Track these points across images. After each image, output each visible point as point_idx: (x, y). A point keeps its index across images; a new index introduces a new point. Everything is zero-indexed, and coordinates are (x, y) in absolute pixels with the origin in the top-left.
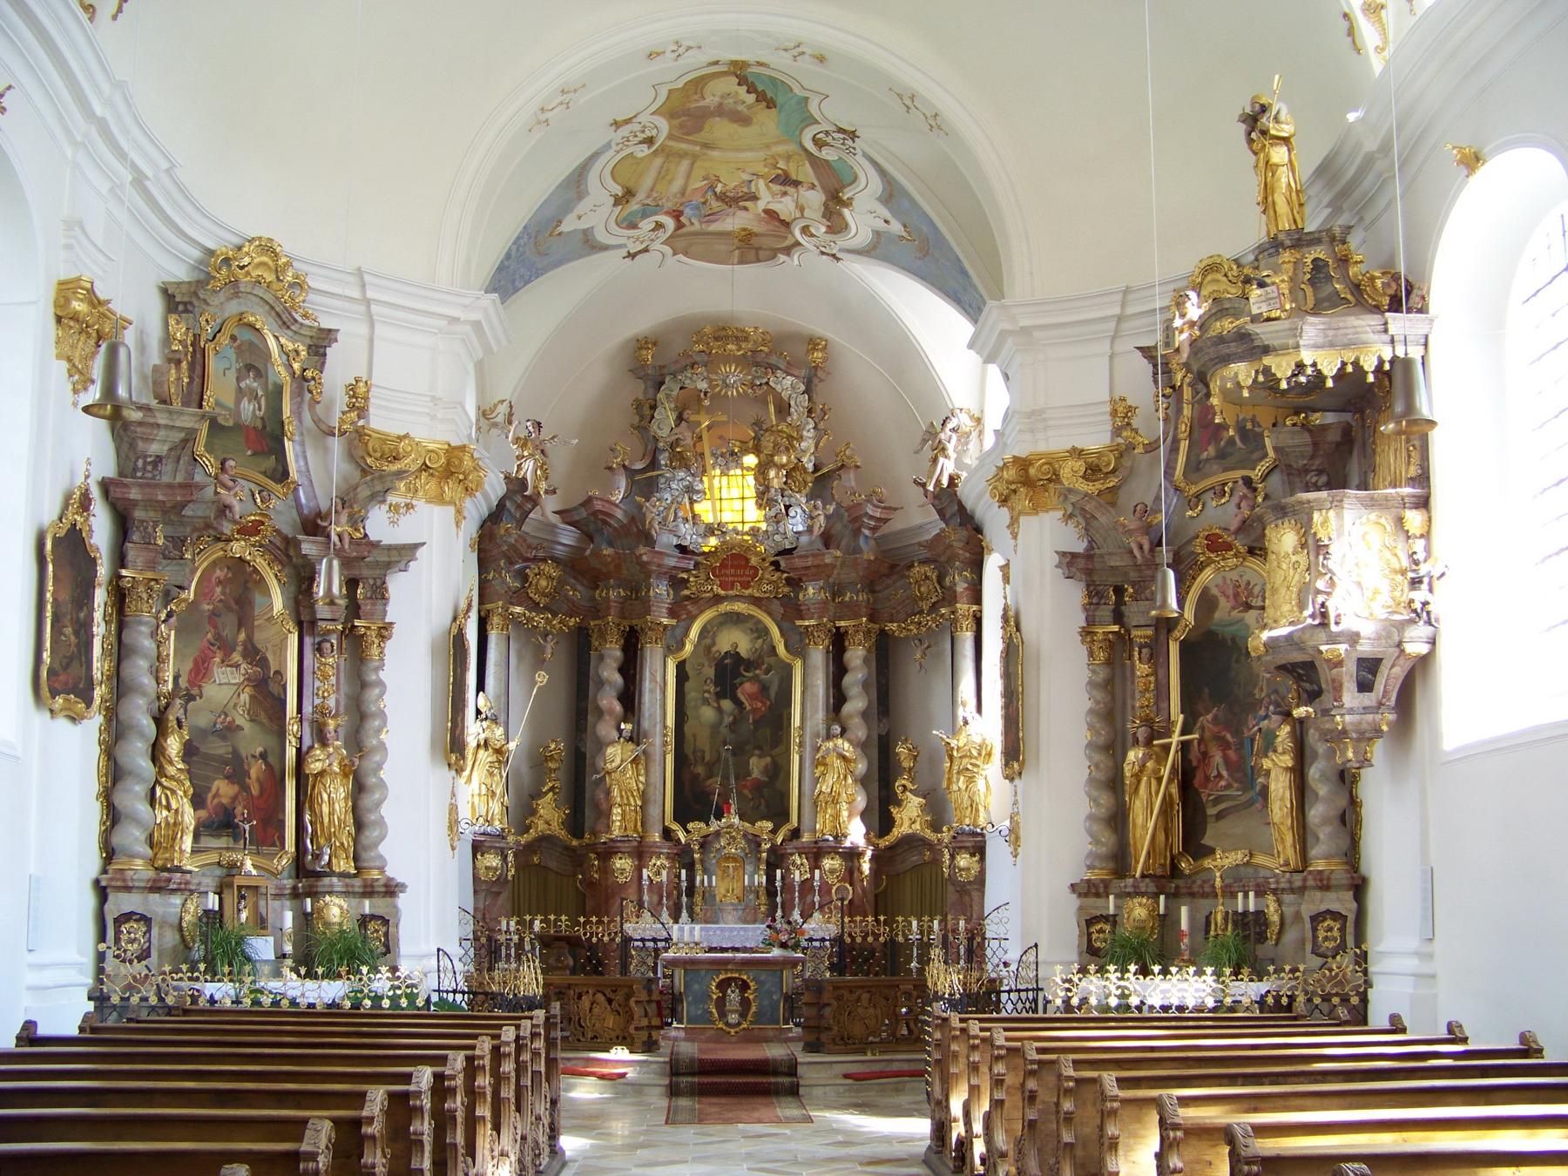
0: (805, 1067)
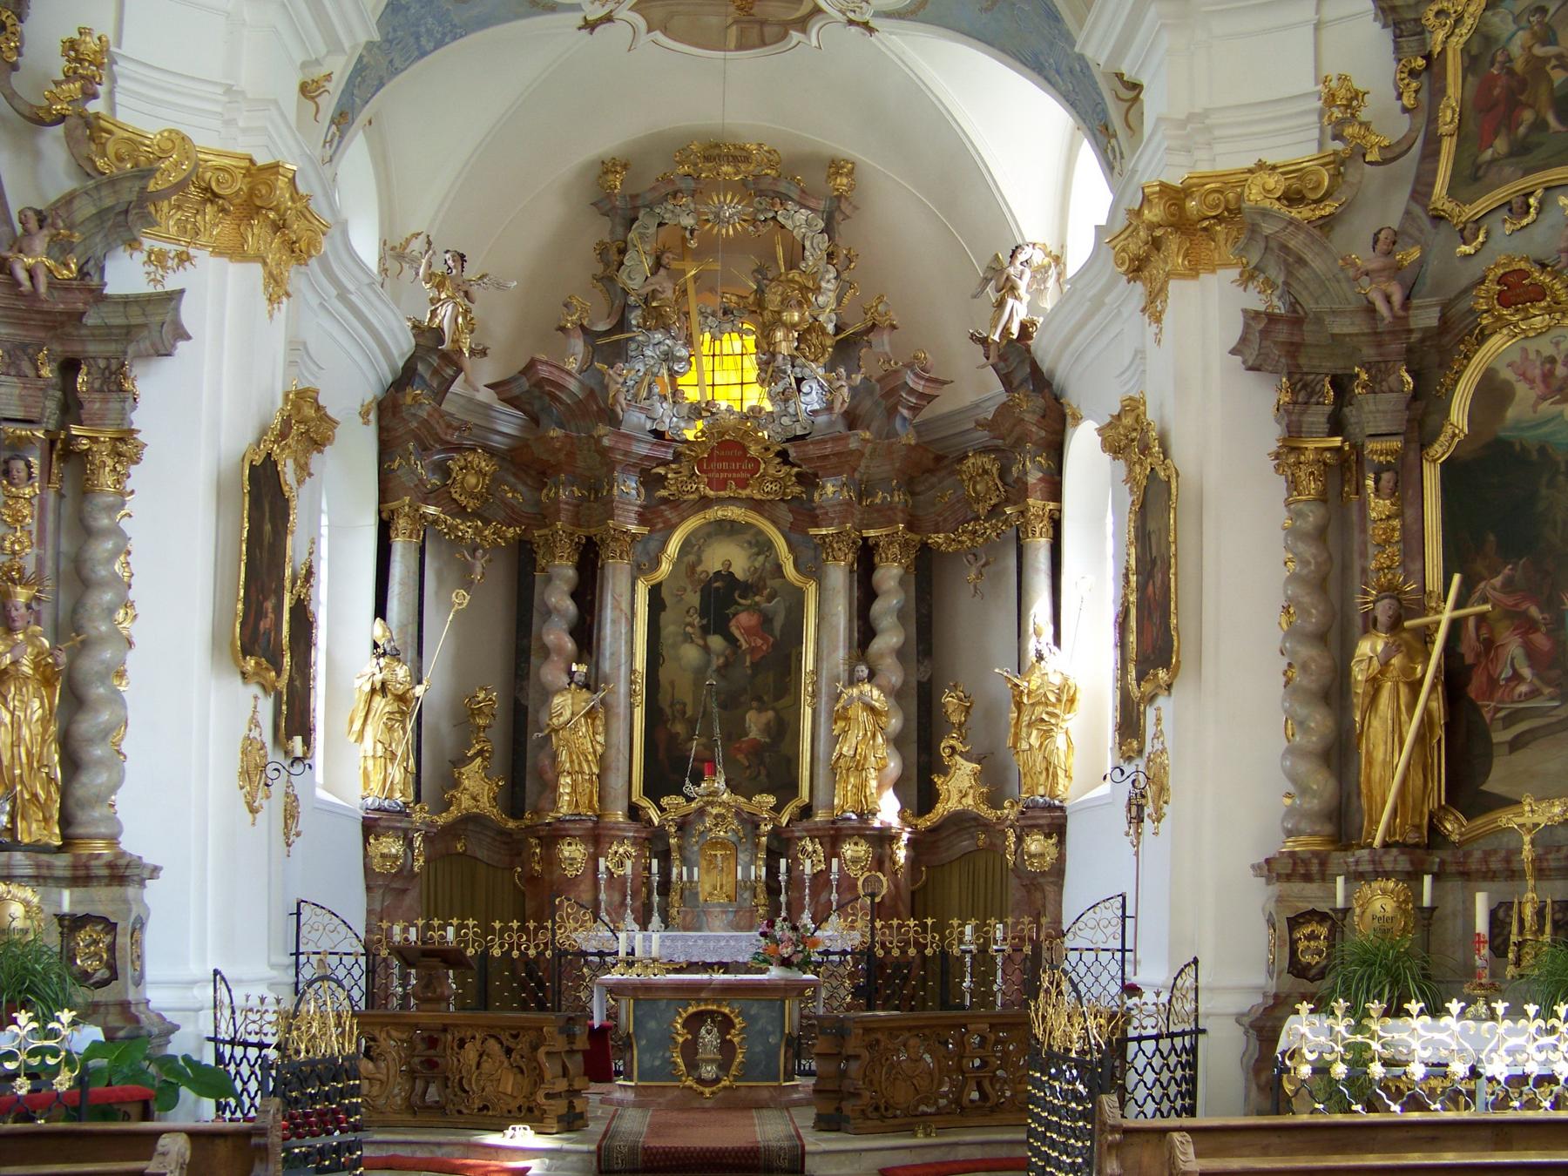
0: (817, 1158)
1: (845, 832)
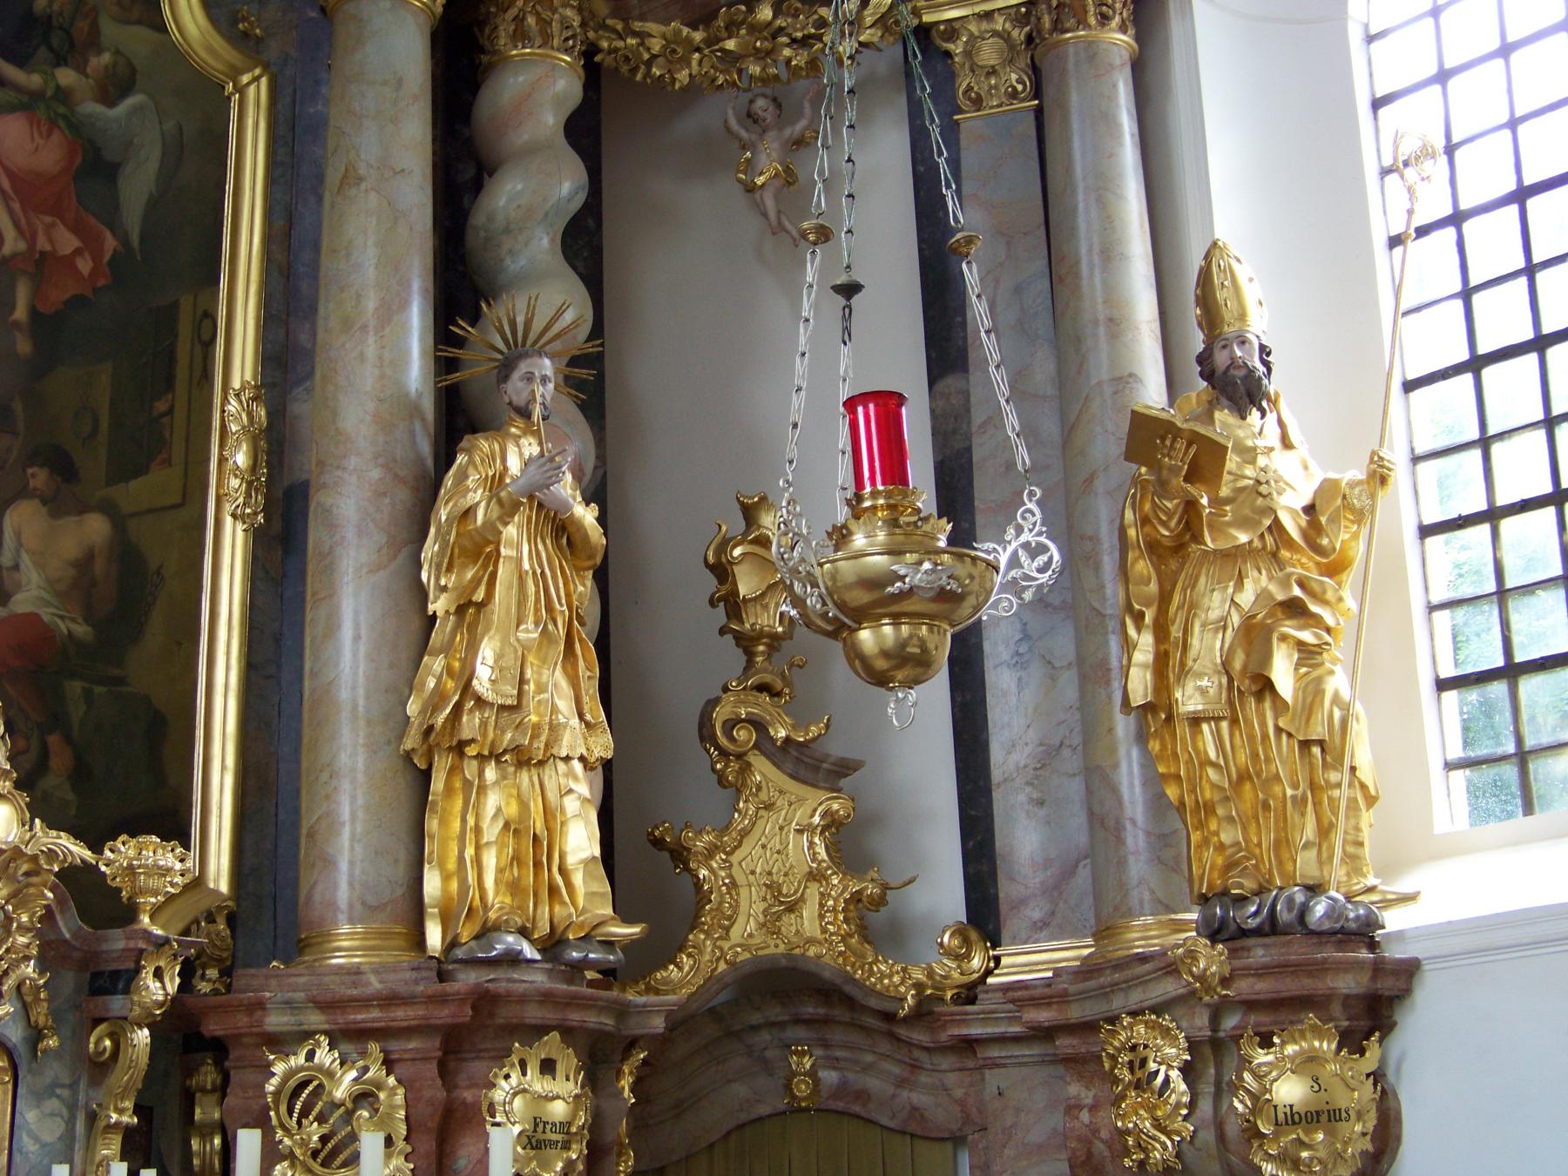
1: (505, 1014)
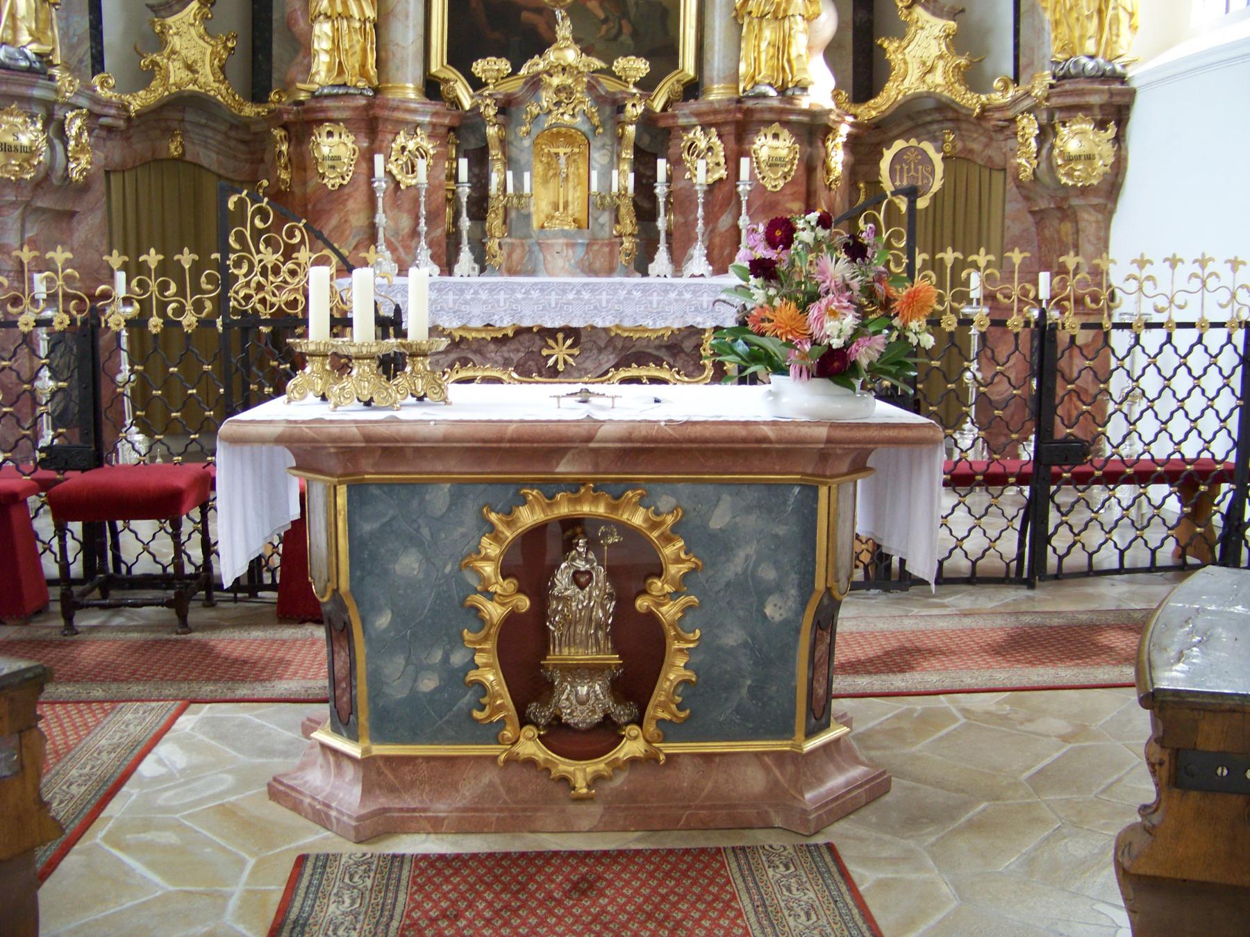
1: (757, 116)
